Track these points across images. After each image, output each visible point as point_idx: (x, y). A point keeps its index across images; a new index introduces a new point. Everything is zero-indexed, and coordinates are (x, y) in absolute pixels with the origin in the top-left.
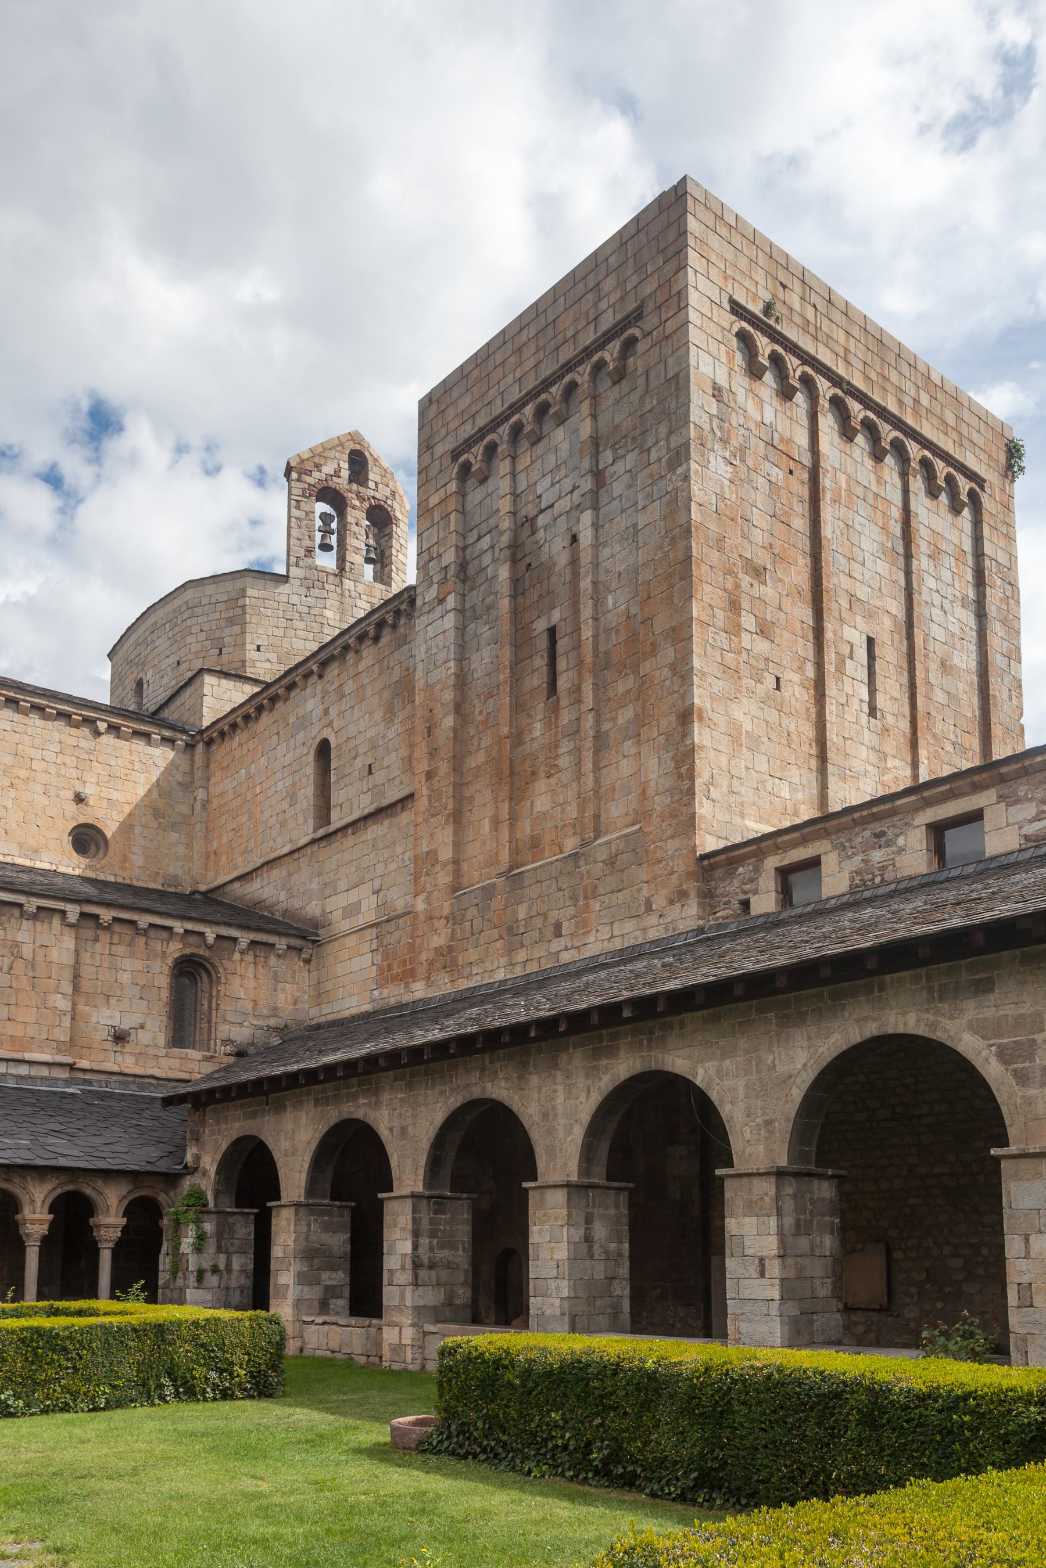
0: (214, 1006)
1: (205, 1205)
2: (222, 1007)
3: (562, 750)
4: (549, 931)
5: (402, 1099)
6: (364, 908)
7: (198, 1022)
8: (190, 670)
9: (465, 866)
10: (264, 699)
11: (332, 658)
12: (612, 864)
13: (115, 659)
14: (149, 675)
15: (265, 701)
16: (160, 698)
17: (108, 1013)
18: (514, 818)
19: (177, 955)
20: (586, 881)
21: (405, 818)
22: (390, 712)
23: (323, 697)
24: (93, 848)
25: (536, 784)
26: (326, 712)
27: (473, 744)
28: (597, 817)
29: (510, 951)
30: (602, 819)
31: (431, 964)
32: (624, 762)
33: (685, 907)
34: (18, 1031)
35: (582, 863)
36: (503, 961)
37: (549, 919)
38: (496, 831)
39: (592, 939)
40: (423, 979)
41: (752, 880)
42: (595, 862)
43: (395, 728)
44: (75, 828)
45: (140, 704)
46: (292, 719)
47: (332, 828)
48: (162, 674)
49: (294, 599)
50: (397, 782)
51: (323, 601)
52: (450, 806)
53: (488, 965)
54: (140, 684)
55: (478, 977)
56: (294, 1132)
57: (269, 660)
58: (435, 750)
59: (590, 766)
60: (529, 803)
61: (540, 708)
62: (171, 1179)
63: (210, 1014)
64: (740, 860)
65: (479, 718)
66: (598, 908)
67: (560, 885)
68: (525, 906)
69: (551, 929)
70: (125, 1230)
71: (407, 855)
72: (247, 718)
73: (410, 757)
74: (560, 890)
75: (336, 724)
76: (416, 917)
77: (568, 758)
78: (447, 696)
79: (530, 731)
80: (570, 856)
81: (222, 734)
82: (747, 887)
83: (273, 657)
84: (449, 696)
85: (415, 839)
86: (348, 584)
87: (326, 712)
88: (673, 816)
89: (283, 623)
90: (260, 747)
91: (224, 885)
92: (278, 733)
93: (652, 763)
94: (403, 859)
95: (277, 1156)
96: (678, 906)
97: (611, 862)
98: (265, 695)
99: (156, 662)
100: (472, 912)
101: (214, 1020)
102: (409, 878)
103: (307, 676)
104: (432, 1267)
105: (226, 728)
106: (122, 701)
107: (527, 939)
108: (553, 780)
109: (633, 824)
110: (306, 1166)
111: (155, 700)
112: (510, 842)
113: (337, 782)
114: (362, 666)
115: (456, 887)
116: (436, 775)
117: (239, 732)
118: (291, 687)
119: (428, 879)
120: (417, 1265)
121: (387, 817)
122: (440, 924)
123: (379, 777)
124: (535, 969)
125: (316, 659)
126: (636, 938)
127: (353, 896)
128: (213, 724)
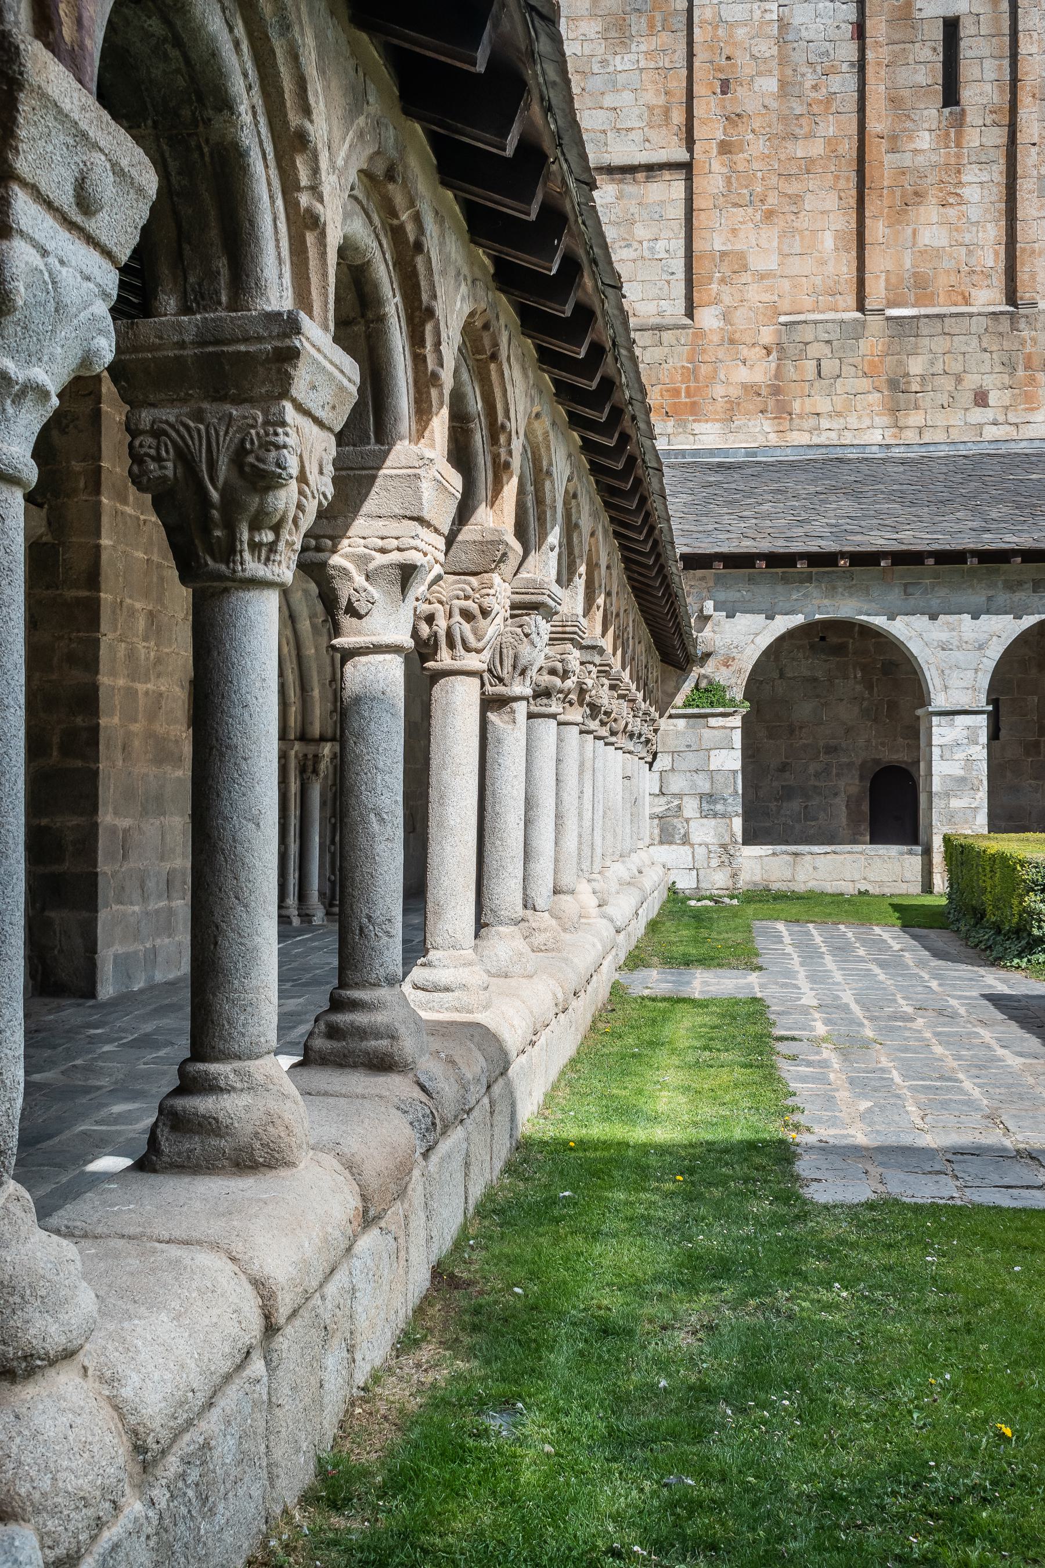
3: (965, 178)
4: (967, 398)
25: (922, 209)
27: (801, 126)
35: (1022, 325)
37: (964, 383)
40: (717, 420)
43: (633, 57)
53: (853, 421)
55: (833, 435)
61: (931, 112)
67: (985, 345)
68: (920, 358)
71: (661, 245)
76: (700, 334)
77: (979, 190)
79: (911, 138)
107: (926, 400)
108: (951, 212)
116: (742, 151)
119: (724, 288)
124: (940, 436)
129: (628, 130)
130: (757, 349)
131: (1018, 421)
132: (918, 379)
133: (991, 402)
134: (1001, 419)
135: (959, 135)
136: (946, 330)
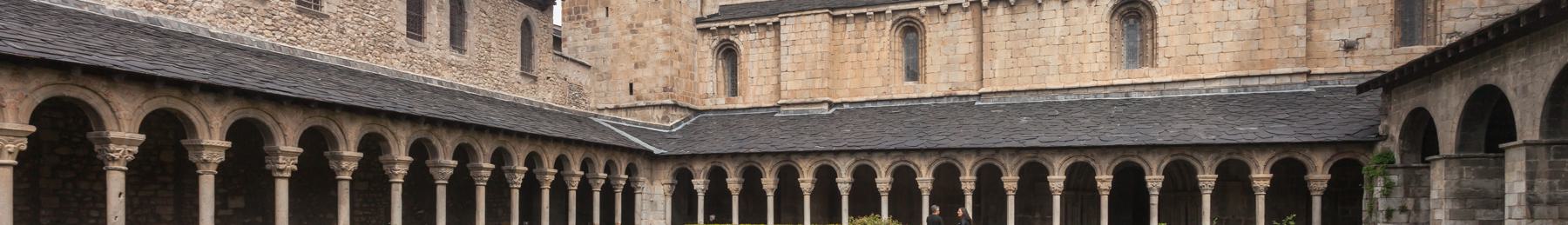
0: (1439, 8)
1: (1393, 162)
2: (1446, 7)
5: (1523, 63)
7: (1425, 22)
17: (1338, 31)
34: (1266, 55)
56: (1447, 100)
62: (1369, 145)
63: (1436, 15)
70: (1330, 182)
95: (1436, 121)
101: (1439, 19)
104: (1551, 203)
110: (1455, 126)
120: (1531, 202)
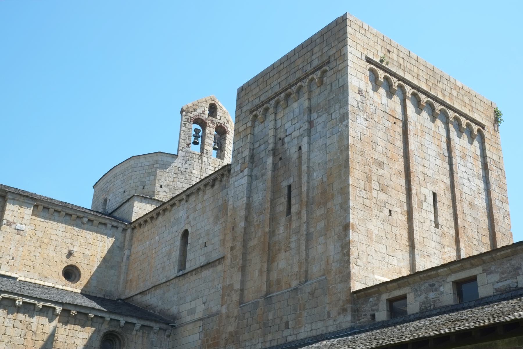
3: (292, 240)
6: (197, 311)
8: (129, 195)
9: (246, 292)
10: (161, 210)
11: (192, 193)
12: (313, 294)
13: (96, 189)
14: (110, 197)
15: (161, 211)
16: (114, 207)
18: (269, 271)
19: (105, 331)
20: (301, 302)
21: (220, 268)
22: (216, 218)
23: (187, 211)
24: (73, 276)
26: (188, 217)
28: (306, 272)
29: (264, 335)
30: (309, 272)
31: (227, 340)
32: (319, 247)
33: (346, 317)
35: (299, 293)
36: (261, 340)
38: (261, 276)
39: (303, 331)
41: (376, 305)
42: (305, 293)
43: (218, 226)
44: (66, 267)
45: (105, 209)
46: (172, 220)
47: (186, 271)
48: (116, 196)
49: (180, 165)
50: (217, 251)
51: (192, 166)
52: (241, 263)
54: (106, 200)
57: (165, 192)
58: (235, 237)
59: (304, 248)
60: (276, 264)
61: (283, 220)
64: (370, 295)
65: (256, 224)
66: (305, 315)
67: (289, 303)
69: (284, 325)
72: (152, 218)
73: (224, 240)
74: (289, 306)
75: (192, 222)
77: (295, 243)
78: (242, 213)
80: (294, 289)
81: (140, 225)
82: (374, 308)
83: (167, 190)
84: (243, 213)
85: (224, 278)
86: (205, 159)
87: (188, 217)
88: (340, 272)
89: (173, 175)
90: (157, 232)
91: (133, 296)
92: (165, 226)
93: (332, 248)
94: (217, 287)
96: (342, 316)
97: (312, 293)
98: (161, 208)
99: (114, 191)
100: (247, 315)
102: (219, 297)
103: (180, 201)
105: (142, 222)
106: (97, 208)
108: (287, 253)
109: (323, 276)
111: (112, 208)
112: (267, 281)
113: (190, 250)
114: (206, 197)
115: (241, 302)
117: (148, 224)
118: (173, 205)
121: (211, 267)
122: (232, 320)
123: (210, 248)
124: (275, 343)
125: (185, 194)
126: (323, 331)
127: (193, 305)
128: (137, 220)
129: (216, 249)
130: (234, 318)
131: (297, 333)
132: (271, 321)
133: (290, 327)
134: (292, 333)
135: (290, 224)
136: (279, 300)
